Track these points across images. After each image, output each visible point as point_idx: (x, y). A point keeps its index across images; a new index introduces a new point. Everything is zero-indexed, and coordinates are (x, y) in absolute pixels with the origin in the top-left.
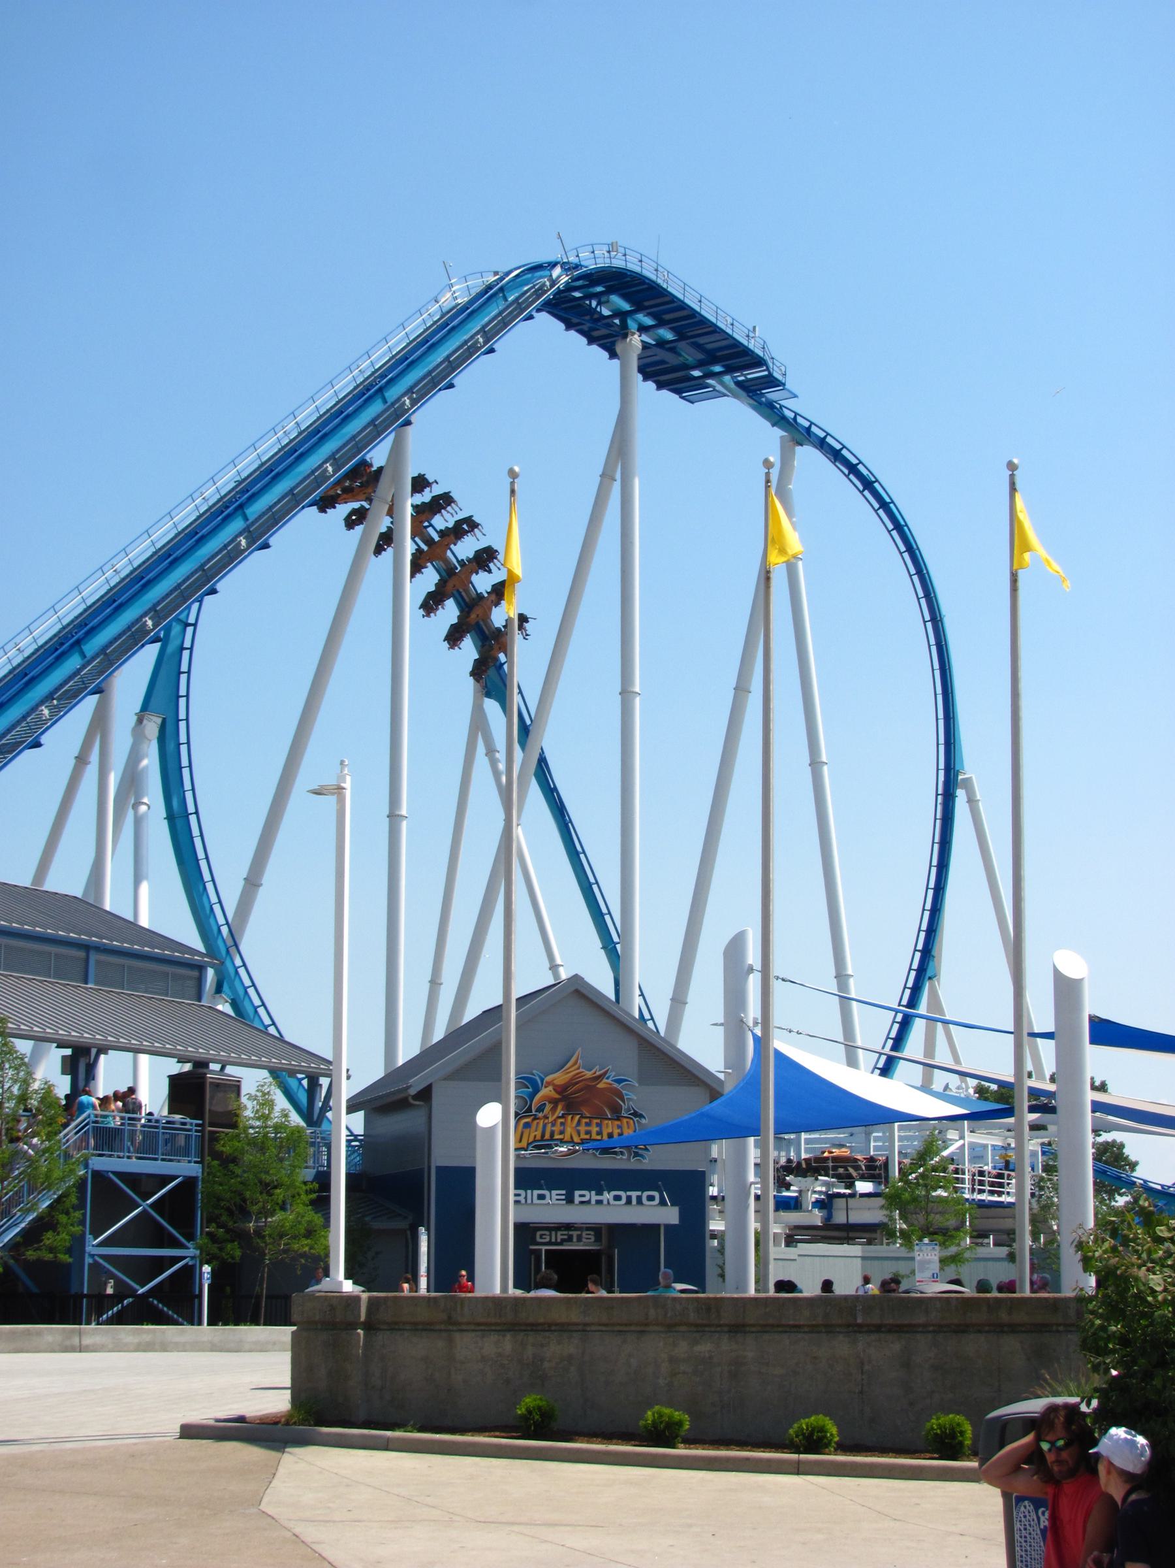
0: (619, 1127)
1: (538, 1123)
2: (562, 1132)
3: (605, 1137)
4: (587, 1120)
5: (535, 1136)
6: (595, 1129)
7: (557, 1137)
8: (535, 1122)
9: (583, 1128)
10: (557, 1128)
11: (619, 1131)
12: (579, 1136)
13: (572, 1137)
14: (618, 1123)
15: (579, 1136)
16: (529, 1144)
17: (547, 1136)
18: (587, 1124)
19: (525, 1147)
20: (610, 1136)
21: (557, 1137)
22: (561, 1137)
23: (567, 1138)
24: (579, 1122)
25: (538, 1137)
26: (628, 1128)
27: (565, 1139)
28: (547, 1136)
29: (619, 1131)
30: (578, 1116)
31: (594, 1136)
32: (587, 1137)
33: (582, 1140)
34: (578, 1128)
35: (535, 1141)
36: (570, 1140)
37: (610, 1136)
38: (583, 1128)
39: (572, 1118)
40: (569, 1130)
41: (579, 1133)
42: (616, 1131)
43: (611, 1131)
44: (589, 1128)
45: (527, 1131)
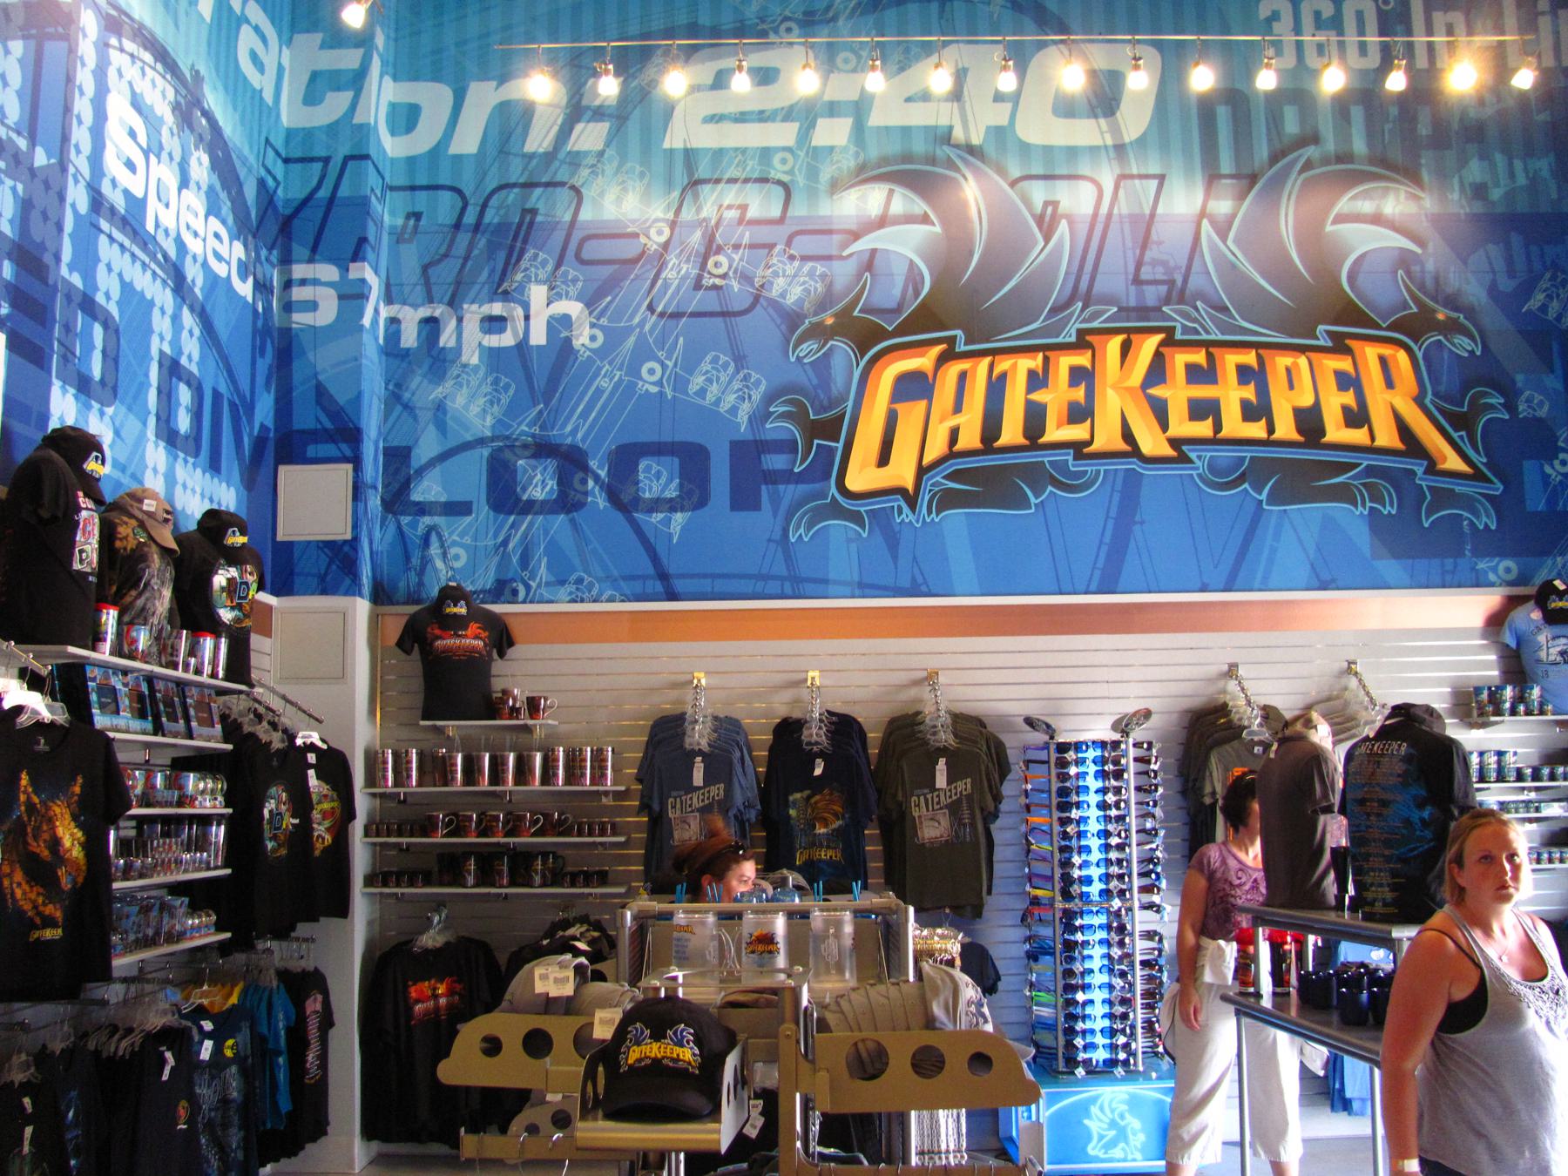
0: (1345, 381)
1: (963, 377)
2: (1079, 413)
3: (1286, 428)
4: (1199, 357)
5: (954, 435)
6: (1232, 395)
7: (1056, 432)
8: (954, 369)
9: (1177, 394)
10: (1057, 396)
11: (1349, 398)
12: (1164, 426)
13: (1128, 436)
14: (1345, 364)
15: (1164, 426)
16: (922, 471)
17: (1012, 432)
18: (1195, 374)
19: (909, 483)
20: (1309, 421)
21: (1056, 432)
22: (1078, 432)
23: (1107, 437)
24: (1158, 358)
25: (970, 438)
26: (1390, 384)
27: (1096, 446)
28: (1012, 432)
29: (1349, 398)
30: (1153, 341)
31: (1234, 425)
32: (1204, 429)
33: (1175, 443)
34: (1153, 391)
35: (951, 455)
36: (1122, 446)
37: (1309, 421)
38: (1177, 394)
39: (1126, 349)
40: (1113, 405)
41: (1160, 412)
42: (1334, 402)
43: (1307, 400)
44: (1203, 392)
45: (911, 415)
